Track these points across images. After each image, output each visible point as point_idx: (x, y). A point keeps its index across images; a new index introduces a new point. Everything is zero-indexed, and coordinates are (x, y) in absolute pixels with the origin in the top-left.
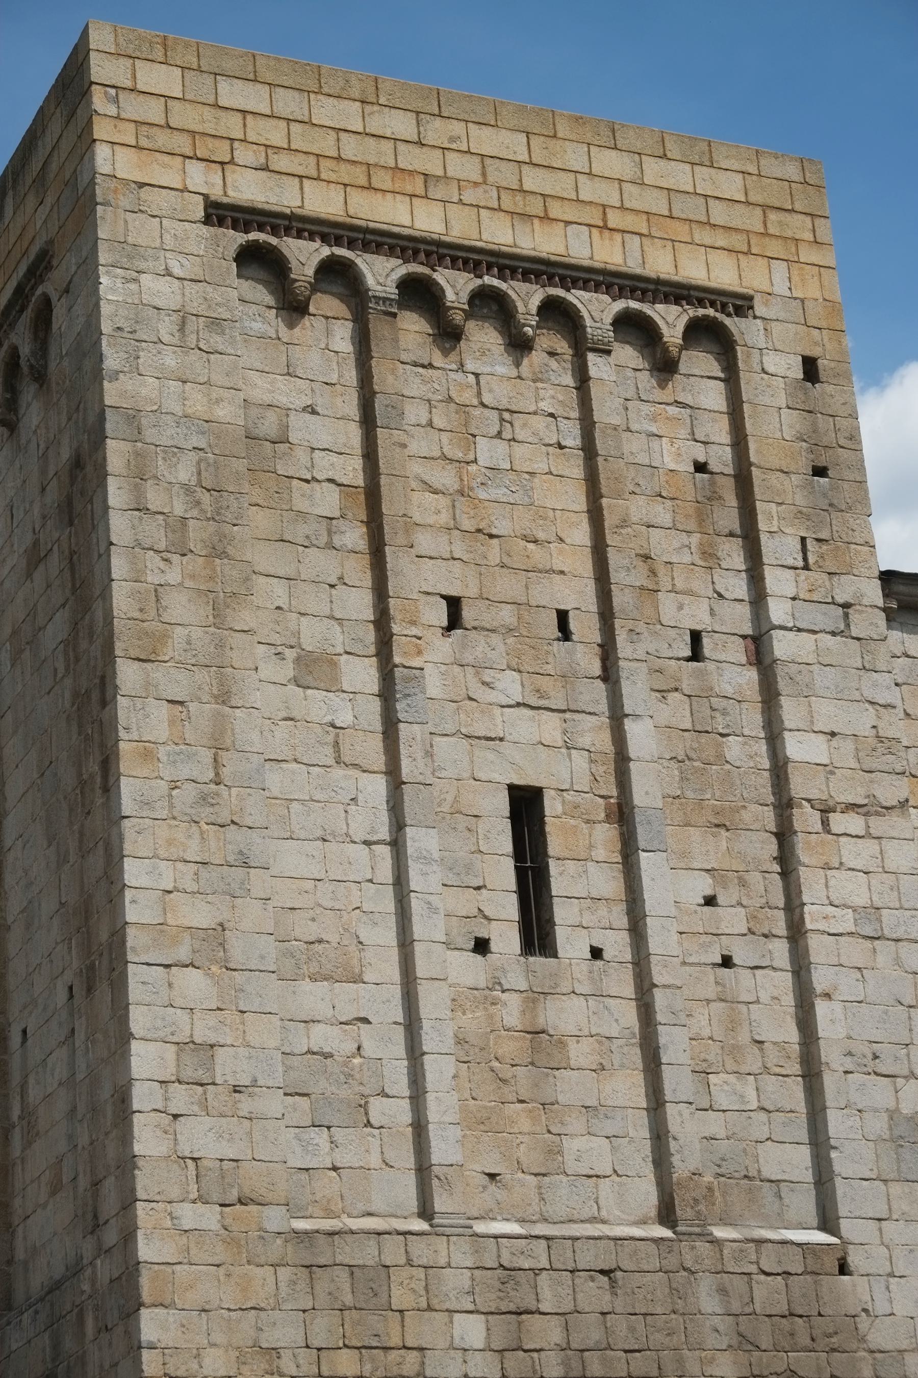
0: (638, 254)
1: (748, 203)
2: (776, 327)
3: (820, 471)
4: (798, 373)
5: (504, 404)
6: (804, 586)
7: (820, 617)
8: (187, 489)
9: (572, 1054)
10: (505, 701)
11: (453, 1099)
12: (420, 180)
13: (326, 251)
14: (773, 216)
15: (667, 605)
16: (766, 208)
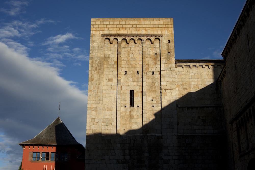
0: (149, 32)
1: (163, 24)
2: (165, 38)
3: (169, 53)
4: (168, 42)
5: (133, 50)
6: (165, 66)
7: (167, 69)
8: (97, 64)
9: (134, 117)
10: (130, 81)
11: (120, 122)
12: (125, 28)
13: (114, 38)
14: (166, 25)
15: (150, 70)
16: (165, 25)
